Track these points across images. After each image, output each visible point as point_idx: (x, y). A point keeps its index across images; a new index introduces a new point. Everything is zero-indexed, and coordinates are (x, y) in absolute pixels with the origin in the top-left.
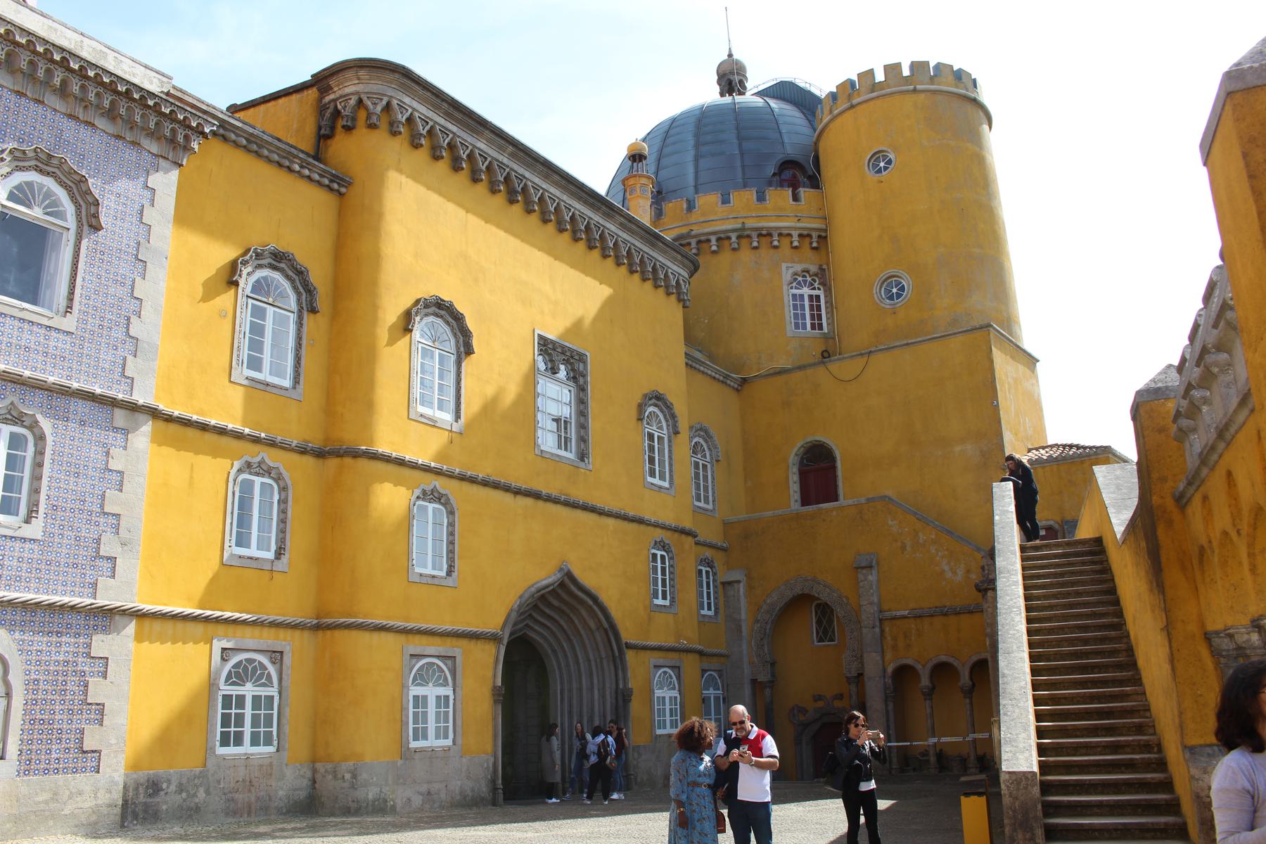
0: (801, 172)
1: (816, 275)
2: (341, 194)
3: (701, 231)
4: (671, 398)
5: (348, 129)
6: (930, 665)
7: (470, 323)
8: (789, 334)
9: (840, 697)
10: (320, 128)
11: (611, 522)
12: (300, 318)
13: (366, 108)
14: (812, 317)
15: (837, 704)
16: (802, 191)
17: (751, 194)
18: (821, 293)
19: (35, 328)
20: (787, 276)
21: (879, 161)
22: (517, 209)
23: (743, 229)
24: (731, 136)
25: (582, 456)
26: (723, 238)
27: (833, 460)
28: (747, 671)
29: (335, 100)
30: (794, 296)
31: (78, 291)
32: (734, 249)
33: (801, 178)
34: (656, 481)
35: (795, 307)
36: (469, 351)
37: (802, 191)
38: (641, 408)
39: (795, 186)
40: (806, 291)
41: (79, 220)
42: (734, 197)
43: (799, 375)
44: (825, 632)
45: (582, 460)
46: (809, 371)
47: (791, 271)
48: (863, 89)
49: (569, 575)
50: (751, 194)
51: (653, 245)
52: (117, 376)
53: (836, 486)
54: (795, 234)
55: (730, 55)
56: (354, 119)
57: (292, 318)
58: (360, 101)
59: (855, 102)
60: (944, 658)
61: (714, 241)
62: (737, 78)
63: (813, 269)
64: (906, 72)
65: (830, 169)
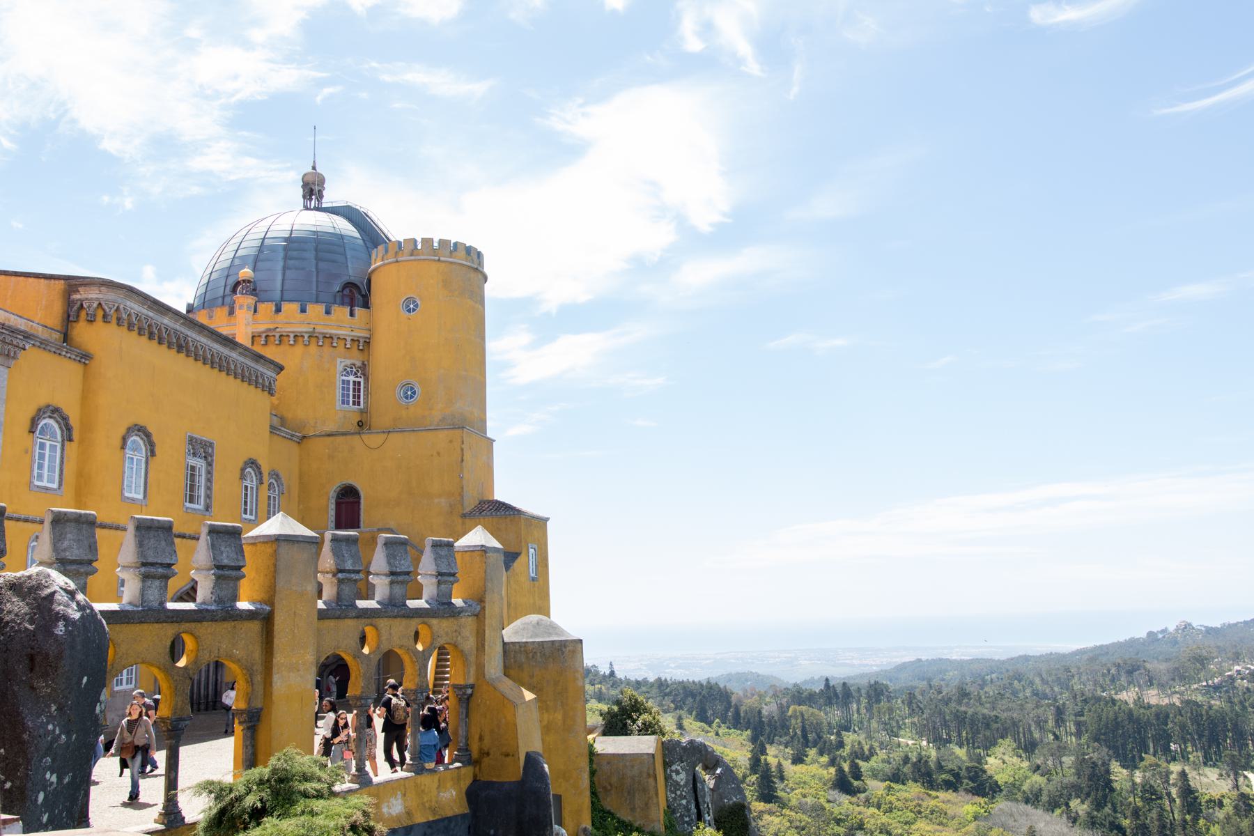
0: (357, 294)
4: (260, 462)
5: (91, 321)
7: (155, 438)
12: (63, 445)
16: (357, 310)
17: (321, 308)
20: (340, 368)
22: (182, 355)
24: (311, 255)
27: (359, 498)
29: (82, 301)
33: (358, 296)
34: (248, 516)
36: (153, 454)
37: (357, 310)
38: (243, 470)
39: (352, 306)
40: (352, 378)
42: (310, 307)
43: (340, 439)
46: (349, 437)
50: (321, 308)
51: (257, 362)
54: (349, 339)
55: (314, 168)
57: (59, 445)
61: (292, 338)
62: (317, 188)
64: (436, 244)
65: (375, 298)
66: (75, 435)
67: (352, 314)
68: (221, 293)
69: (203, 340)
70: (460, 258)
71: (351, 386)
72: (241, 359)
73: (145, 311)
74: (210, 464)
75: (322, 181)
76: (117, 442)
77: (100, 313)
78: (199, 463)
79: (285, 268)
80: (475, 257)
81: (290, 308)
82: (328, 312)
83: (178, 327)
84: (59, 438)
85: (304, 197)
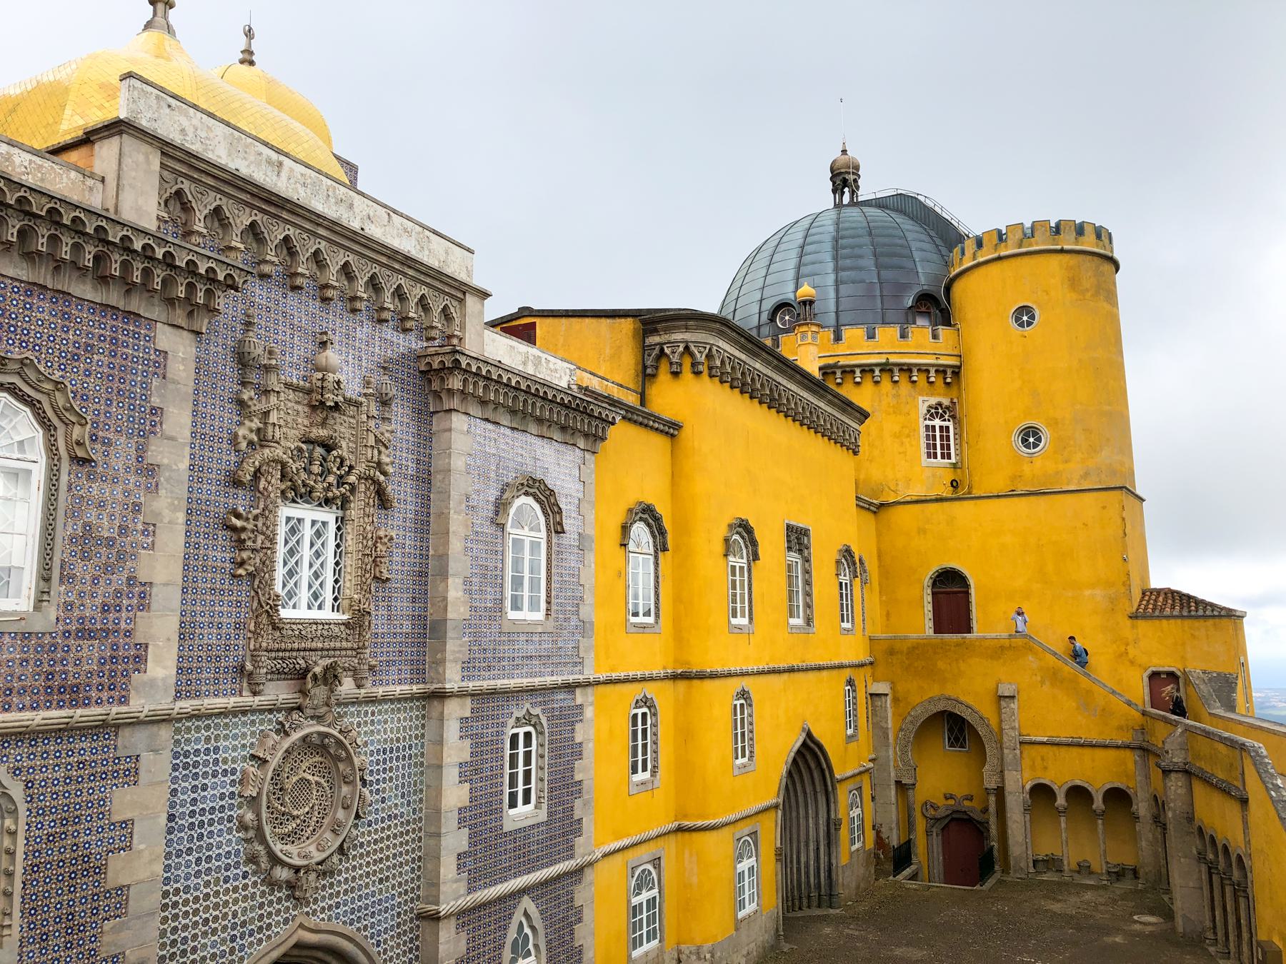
0: (936, 306)
1: (947, 408)
2: (673, 436)
3: (847, 362)
4: (854, 549)
6: (1066, 787)
7: (757, 535)
8: (924, 464)
9: (970, 798)
10: (645, 367)
11: (825, 673)
12: (656, 558)
13: (692, 355)
14: (942, 446)
15: (967, 803)
17: (894, 331)
18: (951, 424)
21: (1024, 315)
23: (887, 364)
24: (869, 262)
25: (809, 621)
26: (867, 370)
27: (968, 586)
28: (893, 774)
29: (661, 344)
30: (927, 427)
32: (877, 383)
35: (928, 436)
36: (756, 557)
40: (937, 422)
41: (548, 530)
42: (880, 332)
44: (957, 739)
45: (808, 625)
46: (946, 504)
47: (927, 404)
48: (1009, 242)
49: (809, 735)
50: (894, 331)
51: (844, 411)
53: (968, 611)
55: (844, 152)
56: (681, 365)
57: (652, 558)
58: (687, 348)
59: (1003, 253)
60: (1078, 783)
62: (852, 177)
63: (946, 402)
66: (670, 545)
67: (935, 337)
68: (755, 323)
69: (793, 387)
70: (1088, 243)
71: (938, 434)
72: (829, 409)
73: (737, 353)
74: (807, 560)
75: (857, 168)
76: (719, 547)
77: (687, 362)
78: (794, 557)
79: (837, 283)
80: (1107, 241)
81: (854, 335)
82: (903, 336)
83: (770, 373)
84: (652, 551)
85: (834, 191)
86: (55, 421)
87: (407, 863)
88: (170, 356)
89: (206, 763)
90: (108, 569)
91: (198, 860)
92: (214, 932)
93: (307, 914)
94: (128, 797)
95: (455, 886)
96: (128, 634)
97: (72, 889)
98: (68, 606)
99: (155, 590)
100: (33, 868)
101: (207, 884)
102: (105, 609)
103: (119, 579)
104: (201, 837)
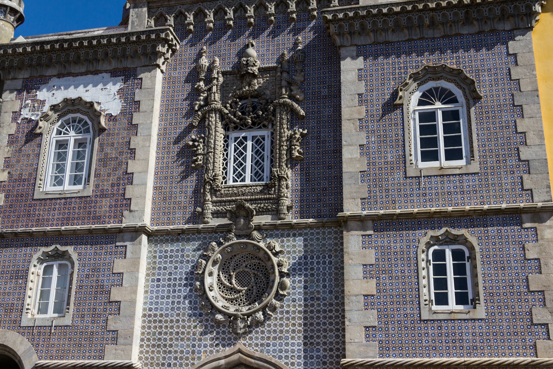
19: (452, 178)
31: (475, 144)
52: (518, 192)
86: (94, 118)
87: (331, 330)
88: (143, 79)
89: (177, 256)
90: (115, 169)
91: (173, 303)
92: (182, 339)
93: (245, 345)
94: (121, 263)
95: (362, 349)
96: (124, 194)
97: (96, 298)
98: (97, 186)
99: (135, 175)
100: (80, 287)
101: (178, 315)
102: (113, 185)
103: (120, 172)
104: (174, 291)
